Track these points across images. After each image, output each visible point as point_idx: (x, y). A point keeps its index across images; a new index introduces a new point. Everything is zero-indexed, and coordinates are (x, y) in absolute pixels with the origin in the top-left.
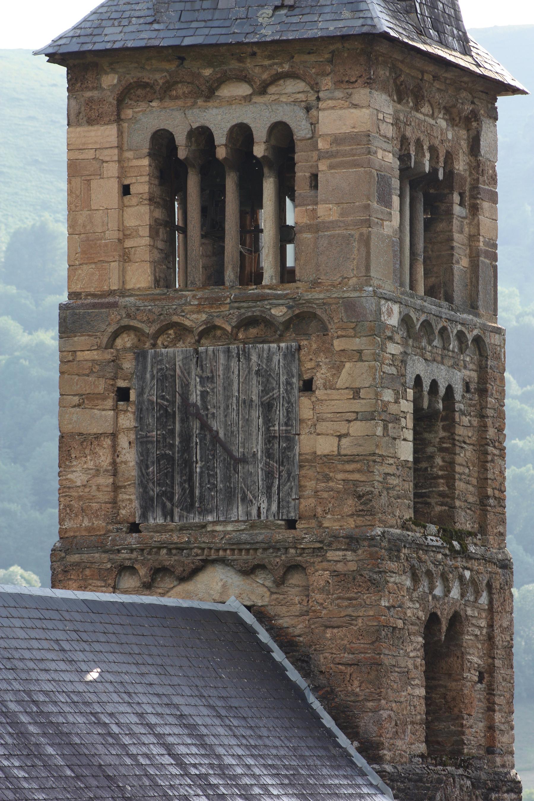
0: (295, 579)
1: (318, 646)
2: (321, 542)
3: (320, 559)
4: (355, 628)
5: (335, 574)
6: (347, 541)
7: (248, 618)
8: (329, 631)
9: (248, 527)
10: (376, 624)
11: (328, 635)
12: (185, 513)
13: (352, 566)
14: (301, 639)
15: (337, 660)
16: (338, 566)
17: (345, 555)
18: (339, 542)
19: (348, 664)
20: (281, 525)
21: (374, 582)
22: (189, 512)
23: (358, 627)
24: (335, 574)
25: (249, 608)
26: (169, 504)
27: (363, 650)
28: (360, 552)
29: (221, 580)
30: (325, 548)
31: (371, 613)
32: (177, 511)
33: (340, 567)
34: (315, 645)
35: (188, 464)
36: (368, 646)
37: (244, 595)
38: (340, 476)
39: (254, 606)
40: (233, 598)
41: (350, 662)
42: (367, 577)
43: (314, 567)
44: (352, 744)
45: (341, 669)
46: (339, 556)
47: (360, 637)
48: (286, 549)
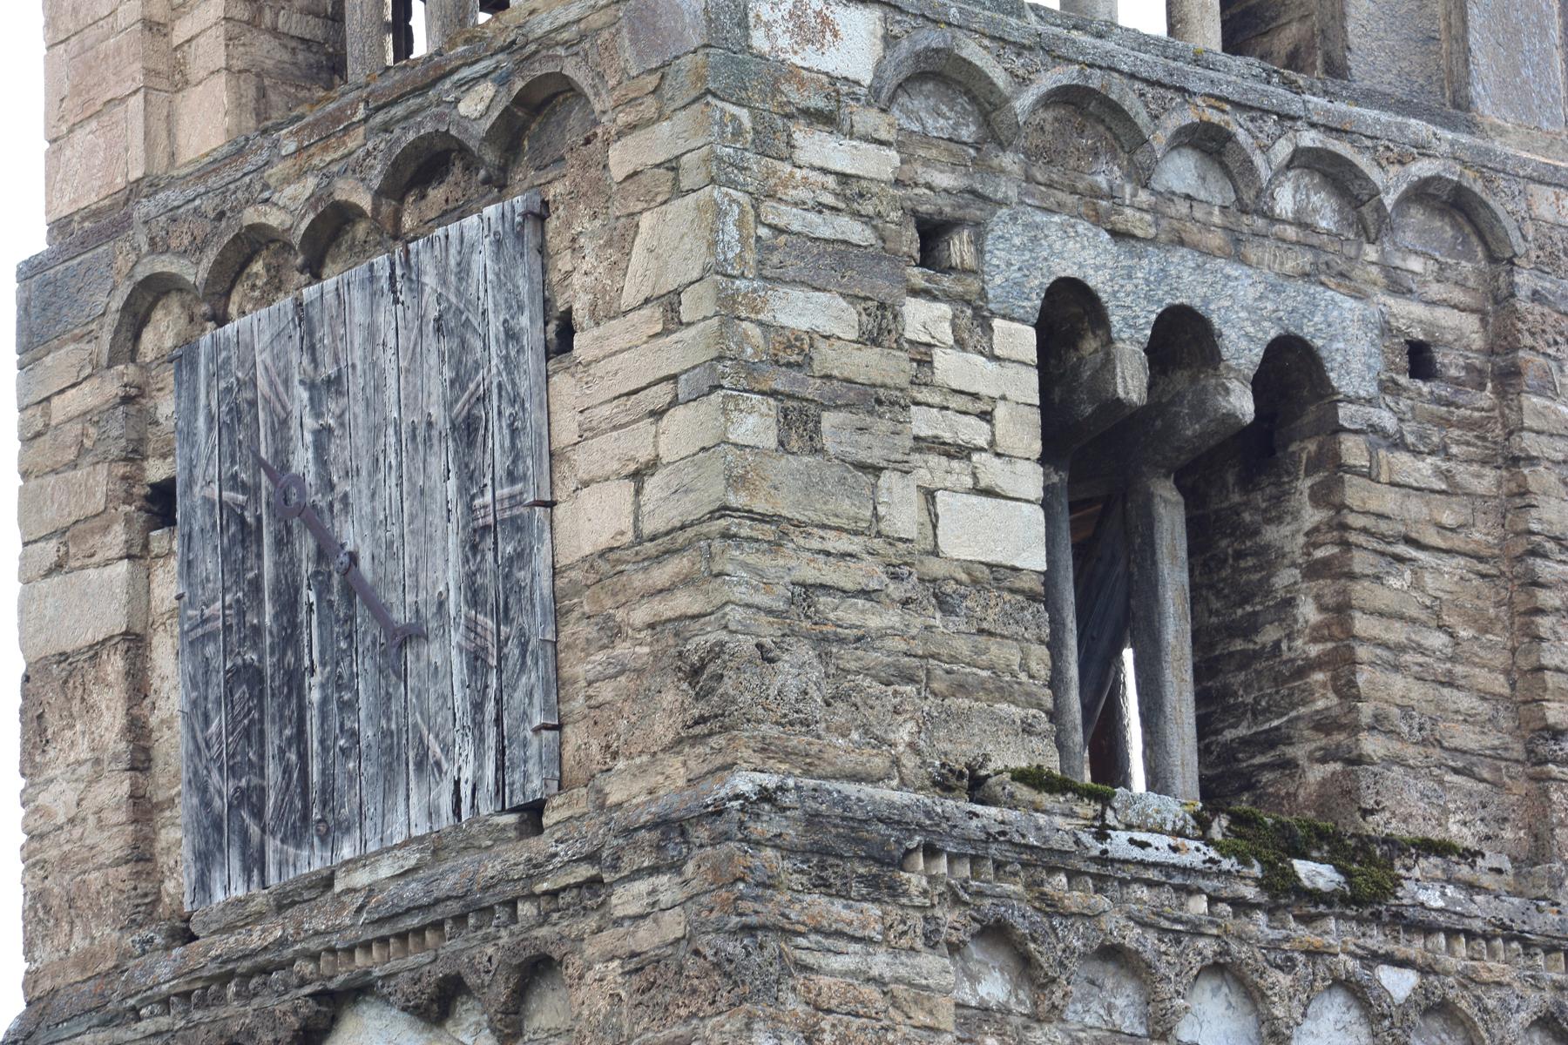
2: (592, 858)
3: (592, 922)
5: (636, 964)
6: (655, 835)
12: (291, 850)
13: (673, 925)
16: (641, 933)
18: (636, 847)
20: (504, 829)
21: (729, 968)
22: (298, 846)
24: (636, 964)
26: (254, 830)
28: (690, 868)
32: (272, 844)
33: (645, 938)
35: (294, 680)
38: (641, 615)
42: (709, 952)
43: (582, 952)
46: (639, 897)
48: (512, 904)
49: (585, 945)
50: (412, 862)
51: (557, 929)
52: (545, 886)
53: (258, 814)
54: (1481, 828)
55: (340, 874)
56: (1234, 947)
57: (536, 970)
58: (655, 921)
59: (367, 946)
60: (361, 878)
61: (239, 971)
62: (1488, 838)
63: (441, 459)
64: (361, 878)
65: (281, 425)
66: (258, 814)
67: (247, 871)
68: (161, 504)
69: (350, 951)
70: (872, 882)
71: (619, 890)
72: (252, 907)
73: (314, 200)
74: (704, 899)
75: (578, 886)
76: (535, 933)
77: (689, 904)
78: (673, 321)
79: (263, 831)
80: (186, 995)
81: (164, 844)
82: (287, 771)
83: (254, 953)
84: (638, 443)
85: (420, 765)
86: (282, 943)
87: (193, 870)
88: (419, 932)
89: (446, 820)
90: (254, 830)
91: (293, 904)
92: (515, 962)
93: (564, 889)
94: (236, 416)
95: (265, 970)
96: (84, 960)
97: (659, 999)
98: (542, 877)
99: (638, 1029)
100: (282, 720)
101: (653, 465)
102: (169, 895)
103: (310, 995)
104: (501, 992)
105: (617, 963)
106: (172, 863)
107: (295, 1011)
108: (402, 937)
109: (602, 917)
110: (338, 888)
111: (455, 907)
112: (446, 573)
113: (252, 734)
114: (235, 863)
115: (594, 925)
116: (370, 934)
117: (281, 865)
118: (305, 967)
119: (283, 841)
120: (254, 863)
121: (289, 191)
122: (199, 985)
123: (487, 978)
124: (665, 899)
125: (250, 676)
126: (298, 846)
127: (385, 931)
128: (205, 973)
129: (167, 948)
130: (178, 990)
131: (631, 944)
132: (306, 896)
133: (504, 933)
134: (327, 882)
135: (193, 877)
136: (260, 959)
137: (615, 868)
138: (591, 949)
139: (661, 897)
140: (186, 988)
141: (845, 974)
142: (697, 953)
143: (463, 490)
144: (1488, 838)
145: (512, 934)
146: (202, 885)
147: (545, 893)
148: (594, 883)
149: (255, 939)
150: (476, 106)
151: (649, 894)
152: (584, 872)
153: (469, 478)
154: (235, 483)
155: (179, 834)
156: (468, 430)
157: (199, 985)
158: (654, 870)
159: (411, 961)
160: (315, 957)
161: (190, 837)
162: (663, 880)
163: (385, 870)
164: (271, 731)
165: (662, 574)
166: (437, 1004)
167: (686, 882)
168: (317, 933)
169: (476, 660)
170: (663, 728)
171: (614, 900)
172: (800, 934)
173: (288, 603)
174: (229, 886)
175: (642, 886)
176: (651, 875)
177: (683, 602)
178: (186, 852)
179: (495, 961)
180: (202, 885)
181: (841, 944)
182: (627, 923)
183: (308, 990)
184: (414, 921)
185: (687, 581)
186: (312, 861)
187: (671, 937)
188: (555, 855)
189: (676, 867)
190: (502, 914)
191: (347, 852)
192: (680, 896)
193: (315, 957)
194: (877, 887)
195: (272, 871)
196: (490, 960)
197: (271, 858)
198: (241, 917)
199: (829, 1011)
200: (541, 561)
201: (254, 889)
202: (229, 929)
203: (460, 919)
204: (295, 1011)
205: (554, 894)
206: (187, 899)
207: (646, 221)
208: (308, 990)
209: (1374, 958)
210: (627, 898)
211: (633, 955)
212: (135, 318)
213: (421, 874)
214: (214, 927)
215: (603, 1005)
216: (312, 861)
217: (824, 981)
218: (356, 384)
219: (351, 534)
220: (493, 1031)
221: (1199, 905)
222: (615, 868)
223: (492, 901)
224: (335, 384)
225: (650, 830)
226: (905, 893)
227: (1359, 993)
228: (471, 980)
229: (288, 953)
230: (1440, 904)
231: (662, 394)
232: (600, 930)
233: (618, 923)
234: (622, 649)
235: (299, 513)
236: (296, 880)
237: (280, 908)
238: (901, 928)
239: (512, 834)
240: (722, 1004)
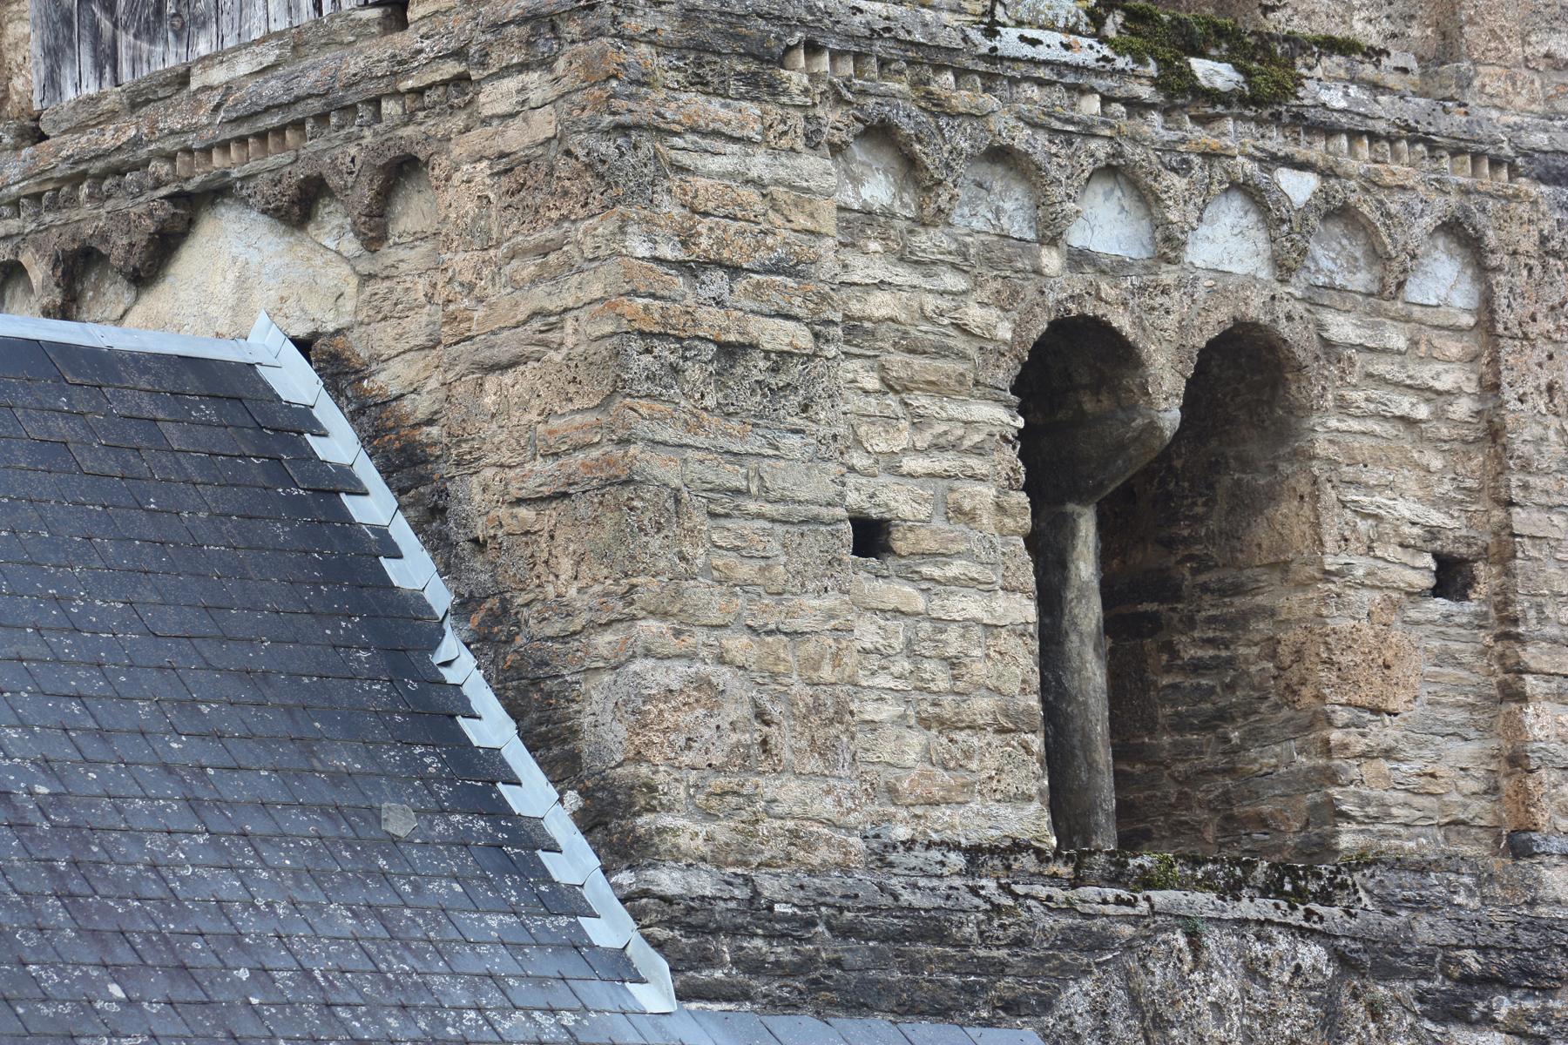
1: (465, 447)
2: (459, 54)
3: (460, 120)
4: (558, 357)
5: (506, 165)
6: (525, 30)
7: (296, 382)
8: (491, 382)
9: (287, 52)
10: (608, 329)
11: (489, 400)
12: (145, 46)
13: (543, 125)
14: (435, 431)
15: (514, 493)
16: (510, 133)
17: (523, 90)
18: (505, 43)
19: (542, 499)
20: (367, 24)
21: (601, 169)
22: (152, 42)
23: (564, 351)
24: (506, 165)
25: (304, 346)
26: (106, 25)
27: (579, 437)
28: (561, 65)
29: (234, 260)
30: (474, 75)
31: (596, 291)
32: (125, 40)
33: (515, 138)
34: (458, 444)
36: (590, 418)
37: (291, 307)
39: (316, 335)
40: (262, 319)
41: (546, 490)
42: (580, 152)
43: (449, 152)
44: (561, 801)
45: (524, 521)
46: (510, 93)
47: (572, 389)
48: (376, 102)
49: (451, 146)
50: (270, 59)
51: (422, 128)
52: (410, 84)
54: (1387, 26)
55: (196, 71)
56: (1128, 148)
57: (402, 170)
58: (525, 120)
59: (225, 146)
60: (218, 75)
61: (91, 171)
62: (1394, 36)
64: (218, 75)
67: (99, 67)
69: (207, 151)
70: (751, 80)
71: (487, 88)
72: (105, 105)
74: (576, 98)
75: (445, 83)
76: (400, 133)
77: (560, 102)
79: (115, 25)
80: (37, 197)
81: (11, 40)
83: (106, 154)
86: (136, 142)
87: (42, 67)
88: (279, 131)
90: (106, 25)
91: (148, 102)
92: (380, 162)
93: (429, 87)
95: (119, 171)
97: (529, 201)
98: (407, 74)
99: (507, 232)
102: (17, 92)
103: (165, 197)
104: (365, 194)
105: (485, 163)
106: (20, 59)
107: (150, 214)
108: (262, 136)
109: (470, 116)
110: (194, 85)
111: (316, 105)
114: (86, 59)
115: (461, 124)
116: (228, 134)
117: (134, 61)
118: (161, 168)
119: (136, 36)
120: (106, 59)
122: (50, 186)
123: (350, 179)
124: (535, 97)
126: (152, 42)
127: (244, 130)
128: (57, 174)
129: (17, 148)
130: (28, 192)
131: (501, 144)
132: (161, 94)
133: (367, 132)
134: (183, 79)
135: (42, 74)
136: (115, 159)
137: (483, 65)
138: (458, 150)
139: (530, 95)
140: (36, 189)
141: (722, 176)
142: (568, 153)
144: (1394, 36)
145: (376, 134)
146: (52, 82)
147: (411, 91)
148: (461, 80)
149: (108, 139)
151: (519, 92)
152: (451, 68)
155: (26, 29)
157: (50, 186)
158: (524, 67)
159: (271, 161)
160: (171, 158)
161: (39, 32)
162: (533, 77)
163: (244, 66)
166: (298, 208)
167: (557, 80)
168: (172, 133)
171: (482, 98)
172: (676, 134)
174: (81, 82)
175: (511, 84)
176: (520, 72)
178: (34, 48)
179: (358, 162)
180: (52, 82)
181: (718, 145)
182: (495, 122)
183: (163, 192)
184: (274, 120)
186: (166, 57)
187: (542, 137)
188: (420, 51)
189: (546, 64)
190: (365, 113)
191: (203, 47)
192: (551, 94)
193: (171, 158)
194: (757, 86)
196: (353, 161)
197: (124, 54)
198: (93, 116)
199: (706, 214)
201: (107, 87)
202: (81, 128)
203: (322, 118)
204: (150, 214)
205: (419, 92)
206: (36, 97)
208: (163, 192)
209: (1273, 161)
210: (496, 97)
211: (502, 155)
213: (281, 71)
214: (65, 126)
215: (471, 207)
216: (166, 57)
217: (701, 182)
220: (357, 235)
221: (1091, 106)
222: (483, 65)
223: (355, 99)
225: (519, 25)
226: (785, 92)
227: (1255, 196)
228: (334, 181)
229: (143, 153)
230: (1343, 104)
232: (468, 129)
233: (486, 122)
236: (150, 77)
237: (134, 106)
238: (782, 128)
239: (375, 29)
240: (594, 206)
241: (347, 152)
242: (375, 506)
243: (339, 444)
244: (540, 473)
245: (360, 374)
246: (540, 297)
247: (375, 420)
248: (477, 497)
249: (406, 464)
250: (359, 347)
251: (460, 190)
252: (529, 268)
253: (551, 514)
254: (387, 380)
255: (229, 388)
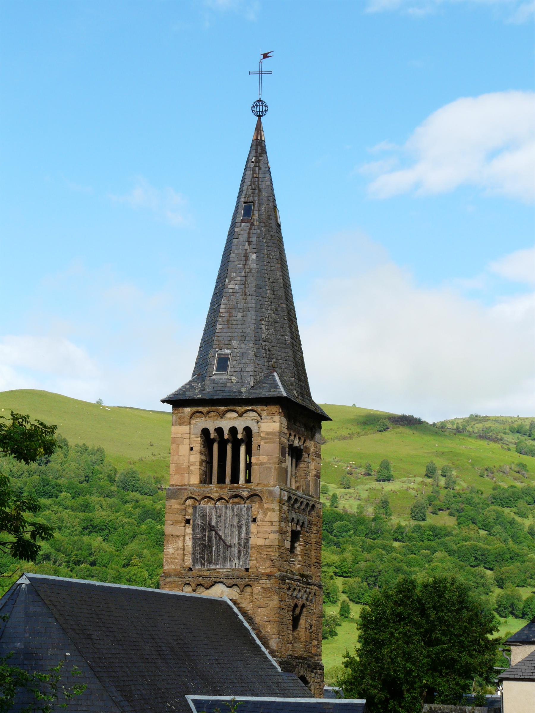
0: (248, 589)
5: (262, 588)
7: (231, 603)
13: (269, 586)
25: (231, 600)
26: (203, 562)
32: (206, 564)
33: (264, 586)
35: (211, 547)
38: (265, 553)
53: (204, 559)
63: (236, 530)
64: (221, 570)
65: (210, 519)
66: (204, 559)
68: (188, 521)
73: (218, 496)
78: (272, 524)
82: (209, 556)
84: (267, 536)
85: (230, 560)
89: (234, 566)
94: (204, 516)
96: (174, 569)
100: (208, 550)
101: (268, 538)
112: (236, 541)
113: (203, 551)
121: (215, 494)
125: (204, 545)
143: (239, 533)
150: (245, 494)
153: (240, 533)
154: (202, 523)
156: (240, 527)
164: (206, 552)
165: (269, 550)
169: (239, 552)
170: (267, 565)
173: (210, 538)
177: (271, 553)
185: (272, 551)
189: (270, 580)
191: (218, 567)
195: (205, 566)
198: (199, 570)
200: (250, 543)
207: (269, 513)
212: (186, 499)
216: (213, 567)
218: (223, 518)
219: (221, 533)
224: (220, 517)
231: (270, 532)
234: (262, 556)
235: (212, 528)
241: (241, 582)
242: (241, 617)
243: (236, 610)
244: (266, 618)
245: (239, 604)
246: (267, 602)
247: (240, 609)
248: (257, 620)
249: (245, 614)
250: (239, 601)
251: (257, 589)
252: (266, 599)
253: (267, 623)
254: (242, 605)
255: (223, 604)
